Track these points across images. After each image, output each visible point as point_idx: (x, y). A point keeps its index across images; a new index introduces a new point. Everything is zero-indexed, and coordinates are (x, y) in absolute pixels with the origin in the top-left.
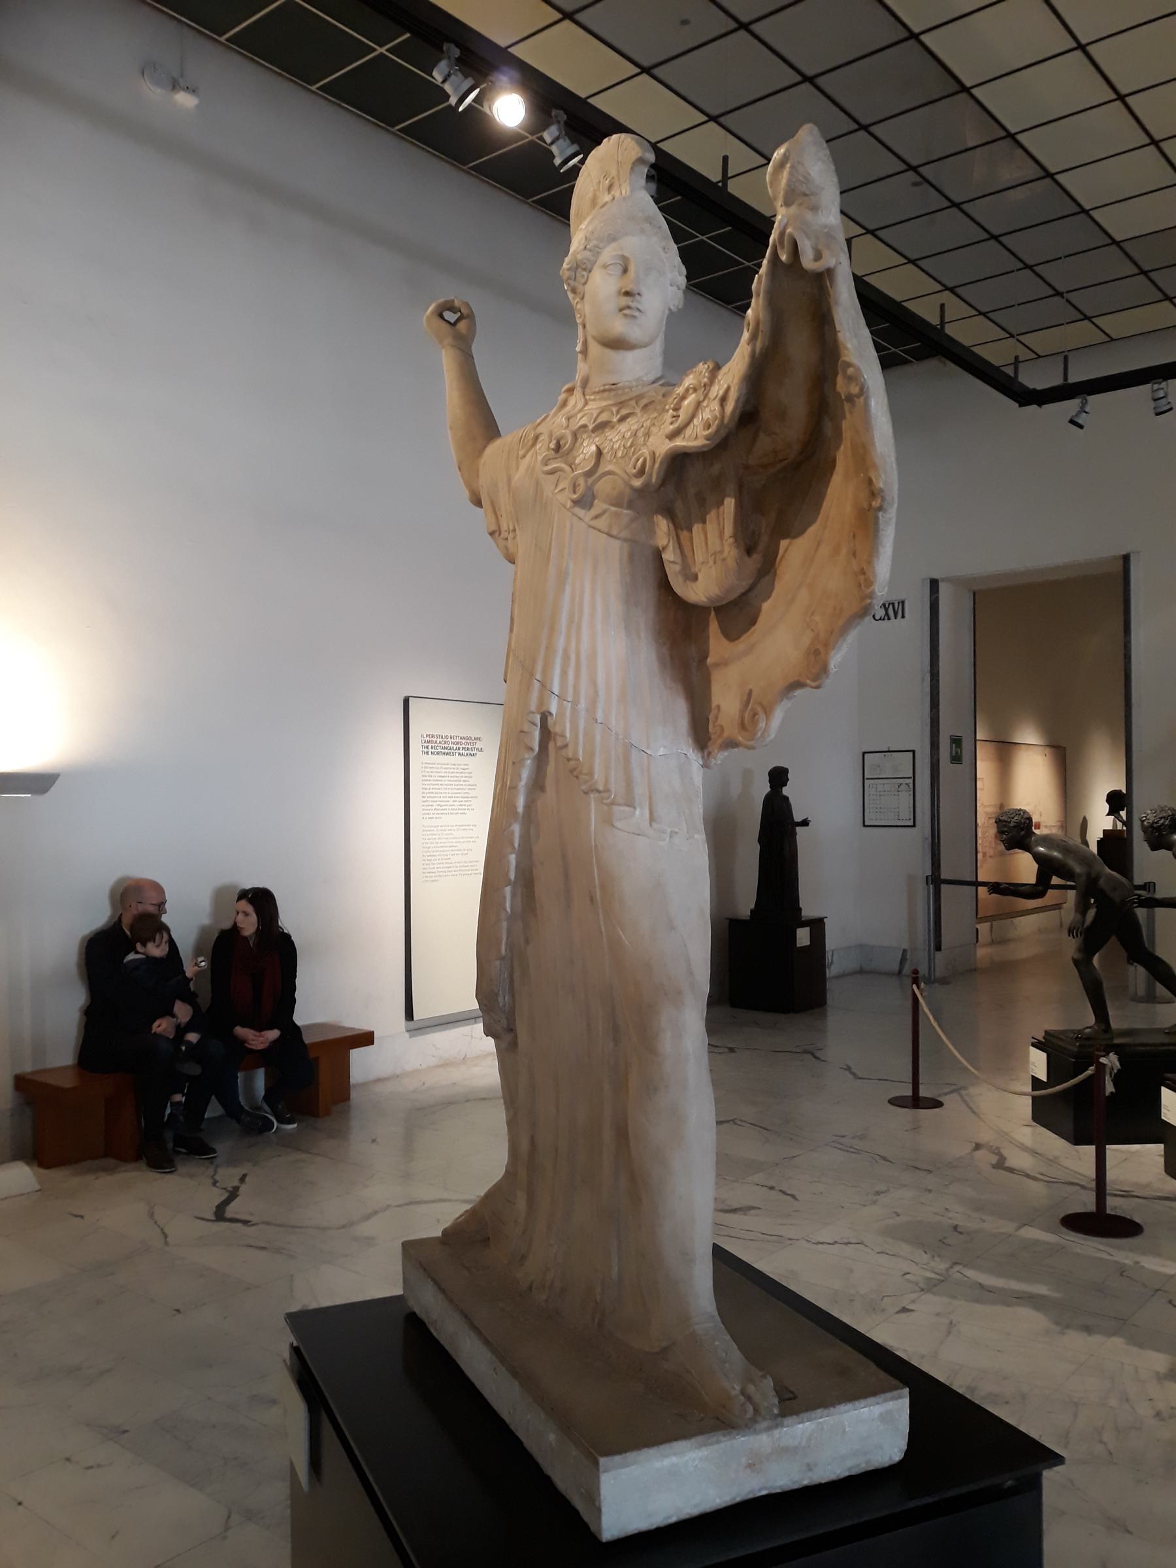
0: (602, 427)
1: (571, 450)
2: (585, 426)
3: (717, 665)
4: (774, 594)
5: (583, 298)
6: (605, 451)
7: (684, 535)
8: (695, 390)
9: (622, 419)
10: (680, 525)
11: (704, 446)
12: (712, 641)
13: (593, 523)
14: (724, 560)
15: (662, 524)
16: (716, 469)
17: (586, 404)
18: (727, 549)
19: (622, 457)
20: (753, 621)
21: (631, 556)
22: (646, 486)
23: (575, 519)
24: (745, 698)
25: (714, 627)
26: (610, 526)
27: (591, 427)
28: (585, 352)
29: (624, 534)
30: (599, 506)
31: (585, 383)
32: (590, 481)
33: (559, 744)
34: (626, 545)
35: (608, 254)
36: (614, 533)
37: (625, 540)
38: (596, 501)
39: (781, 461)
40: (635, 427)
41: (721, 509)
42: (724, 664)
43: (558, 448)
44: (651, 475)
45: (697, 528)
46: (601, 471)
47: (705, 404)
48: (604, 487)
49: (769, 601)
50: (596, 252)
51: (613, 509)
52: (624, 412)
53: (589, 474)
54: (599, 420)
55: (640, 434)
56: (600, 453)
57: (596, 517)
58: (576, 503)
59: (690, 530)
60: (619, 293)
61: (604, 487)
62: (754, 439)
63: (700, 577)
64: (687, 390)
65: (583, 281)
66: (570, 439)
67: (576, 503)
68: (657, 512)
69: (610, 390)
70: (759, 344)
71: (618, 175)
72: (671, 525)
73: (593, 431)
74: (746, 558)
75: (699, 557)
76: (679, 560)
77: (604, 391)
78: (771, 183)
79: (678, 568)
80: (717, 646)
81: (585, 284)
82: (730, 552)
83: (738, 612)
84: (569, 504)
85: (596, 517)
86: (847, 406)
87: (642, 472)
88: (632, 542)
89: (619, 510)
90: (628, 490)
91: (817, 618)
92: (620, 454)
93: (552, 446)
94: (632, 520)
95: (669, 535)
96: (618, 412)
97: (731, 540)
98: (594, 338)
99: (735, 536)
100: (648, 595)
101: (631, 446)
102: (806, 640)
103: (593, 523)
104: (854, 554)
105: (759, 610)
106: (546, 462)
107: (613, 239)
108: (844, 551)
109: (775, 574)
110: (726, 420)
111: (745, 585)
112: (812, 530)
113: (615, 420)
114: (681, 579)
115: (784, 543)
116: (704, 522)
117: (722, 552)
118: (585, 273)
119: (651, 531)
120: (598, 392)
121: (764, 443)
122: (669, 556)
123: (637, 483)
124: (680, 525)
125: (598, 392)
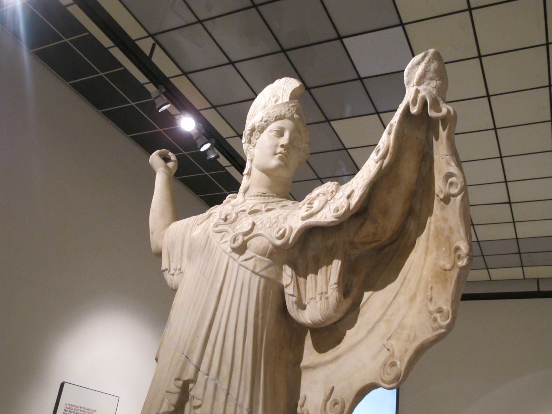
0: (253, 212)
1: (234, 221)
2: (244, 211)
3: (307, 368)
4: (356, 325)
5: (254, 146)
6: (258, 224)
7: (301, 280)
8: (324, 194)
9: (268, 210)
11: (332, 222)
12: (306, 352)
13: (244, 263)
14: (327, 298)
16: (330, 242)
17: (245, 201)
18: (330, 291)
19: (269, 228)
20: (339, 341)
21: (265, 287)
22: (285, 244)
23: (231, 259)
24: (329, 392)
25: (308, 342)
26: (255, 266)
27: (248, 211)
29: (264, 273)
30: (248, 254)
32: (246, 238)
33: (197, 403)
34: (262, 280)
35: (274, 126)
36: (257, 270)
37: (262, 276)
38: (247, 251)
39: (375, 241)
40: (276, 215)
41: (330, 266)
43: (226, 220)
44: (289, 239)
45: (310, 277)
46: (253, 233)
47: (332, 201)
49: (353, 330)
50: (267, 123)
51: (259, 256)
52: (269, 207)
53: (245, 234)
54: (253, 209)
55: (280, 218)
56: (254, 224)
57: (246, 260)
58: (234, 250)
59: (306, 278)
60: (276, 146)
61: (255, 244)
62: (362, 225)
63: (308, 307)
64: (318, 195)
65: (257, 137)
66: (234, 215)
67: (234, 250)
68: (285, 263)
69: (261, 196)
70: (386, 161)
71: (283, 96)
72: (294, 273)
73: (250, 213)
74: (342, 299)
76: (296, 294)
77: (257, 196)
78: (408, 73)
79: (294, 299)
80: (310, 355)
81: (257, 139)
82: (333, 294)
83: (328, 335)
84: (229, 250)
85: (246, 260)
86: (437, 205)
87: (283, 236)
88: (267, 279)
89: (263, 258)
90: (271, 246)
91: (392, 342)
92: (267, 226)
93: (223, 217)
94: (270, 266)
95: (292, 278)
96: (265, 206)
97: (336, 286)
98: (257, 167)
99: (338, 283)
100: (271, 314)
101: (275, 223)
103: (244, 263)
104: (431, 300)
105: (344, 334)
107: (279, 118)
108: (419, 298)
109: (358, 312)
110: (351, 207)
111: (339, 316)
112: (392, 287)
113: (264, 210)
114: (295, 307)
115: (367, 294)
116: (316, 273)
117: (326, 293)
118: (258, 133)
119: (280, 275)
120: (254, 196)
121: (369, 228)
122: (289, 291)
123: (279, 242)
125: (254, 196)
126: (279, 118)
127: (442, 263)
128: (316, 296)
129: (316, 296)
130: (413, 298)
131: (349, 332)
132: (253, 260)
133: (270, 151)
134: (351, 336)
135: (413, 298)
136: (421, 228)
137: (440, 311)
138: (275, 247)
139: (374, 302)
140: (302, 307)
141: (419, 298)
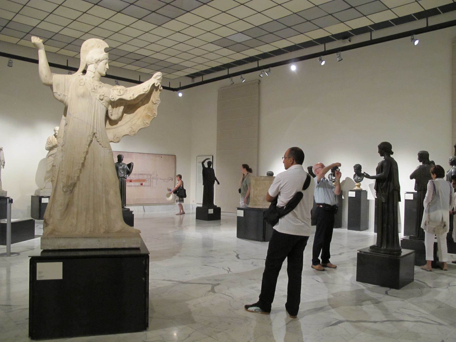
10: (113, 107)
15: (110, 106)
28: (94, 73)
30: (103, 101)
31: (93, 77)
42: (109, 129)
45: (115, 109)
48: (106, 99)
53: (103, 95)
75: (114, 113)
84: (98, 98)
98: (98, 72)
102: (130, 129)
106: (92, 89)
108: (140, 119)
115: (125, 114)
116: (116, 108)
123: (112, 100)
124: (113, 107)
126: (106, 59)
127: (149, 114)
128: (115, 113)
129: (115, 113)
130: (139, 119)
131: (119, 122)
132: (104, 103)
133: (104, 69)
134: (120, 123)
135: (139, 119)
136: (143, 104)
137: (147, 123)
138: (110, 101)
139: (127, 117)
140: (112, 115)
141: (140, 119)
